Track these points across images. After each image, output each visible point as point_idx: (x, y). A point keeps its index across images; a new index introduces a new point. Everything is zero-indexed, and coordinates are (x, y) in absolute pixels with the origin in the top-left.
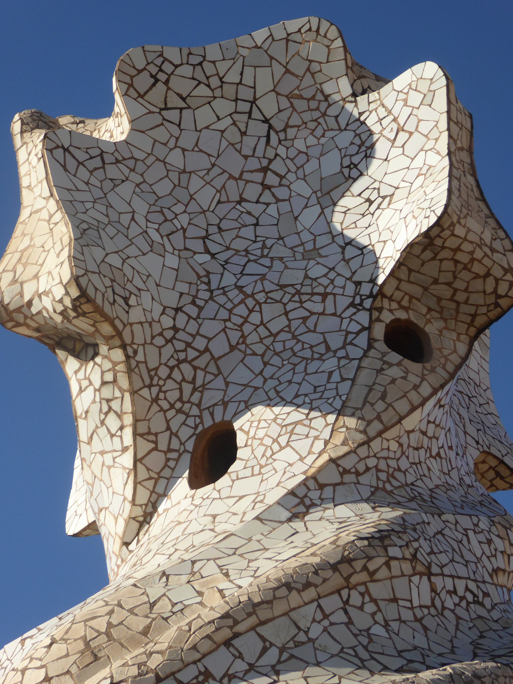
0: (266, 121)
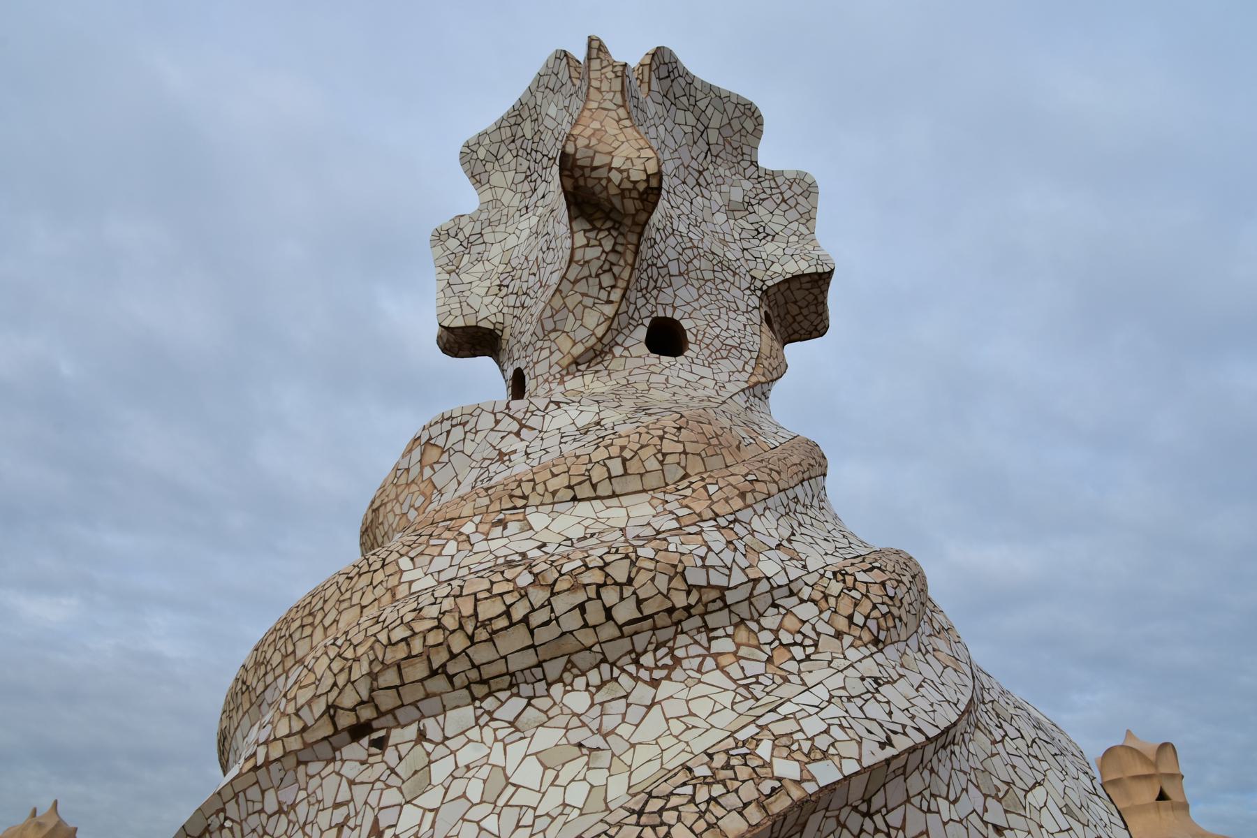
0: (708, 144)
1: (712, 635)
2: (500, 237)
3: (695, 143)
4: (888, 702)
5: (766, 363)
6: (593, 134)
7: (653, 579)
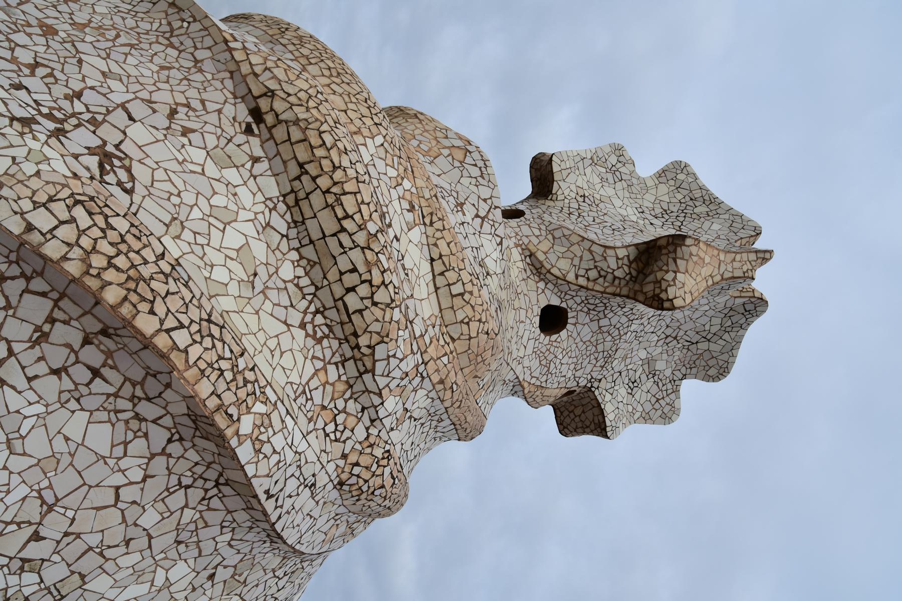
0: (697, 343)
1: (340, 365)
2: (620, 193)
3: (697, 333)
4: (298, 495)
5: (538, 393)
6: (700, 258)
7: (377, 320)
